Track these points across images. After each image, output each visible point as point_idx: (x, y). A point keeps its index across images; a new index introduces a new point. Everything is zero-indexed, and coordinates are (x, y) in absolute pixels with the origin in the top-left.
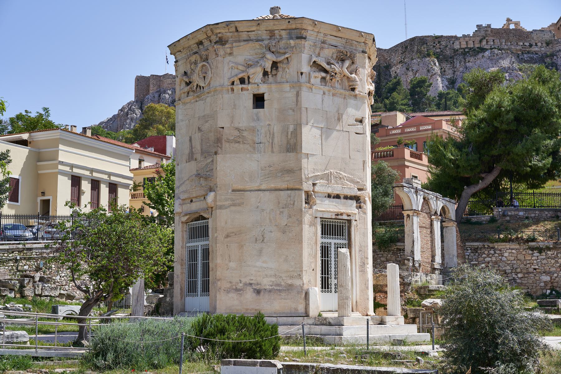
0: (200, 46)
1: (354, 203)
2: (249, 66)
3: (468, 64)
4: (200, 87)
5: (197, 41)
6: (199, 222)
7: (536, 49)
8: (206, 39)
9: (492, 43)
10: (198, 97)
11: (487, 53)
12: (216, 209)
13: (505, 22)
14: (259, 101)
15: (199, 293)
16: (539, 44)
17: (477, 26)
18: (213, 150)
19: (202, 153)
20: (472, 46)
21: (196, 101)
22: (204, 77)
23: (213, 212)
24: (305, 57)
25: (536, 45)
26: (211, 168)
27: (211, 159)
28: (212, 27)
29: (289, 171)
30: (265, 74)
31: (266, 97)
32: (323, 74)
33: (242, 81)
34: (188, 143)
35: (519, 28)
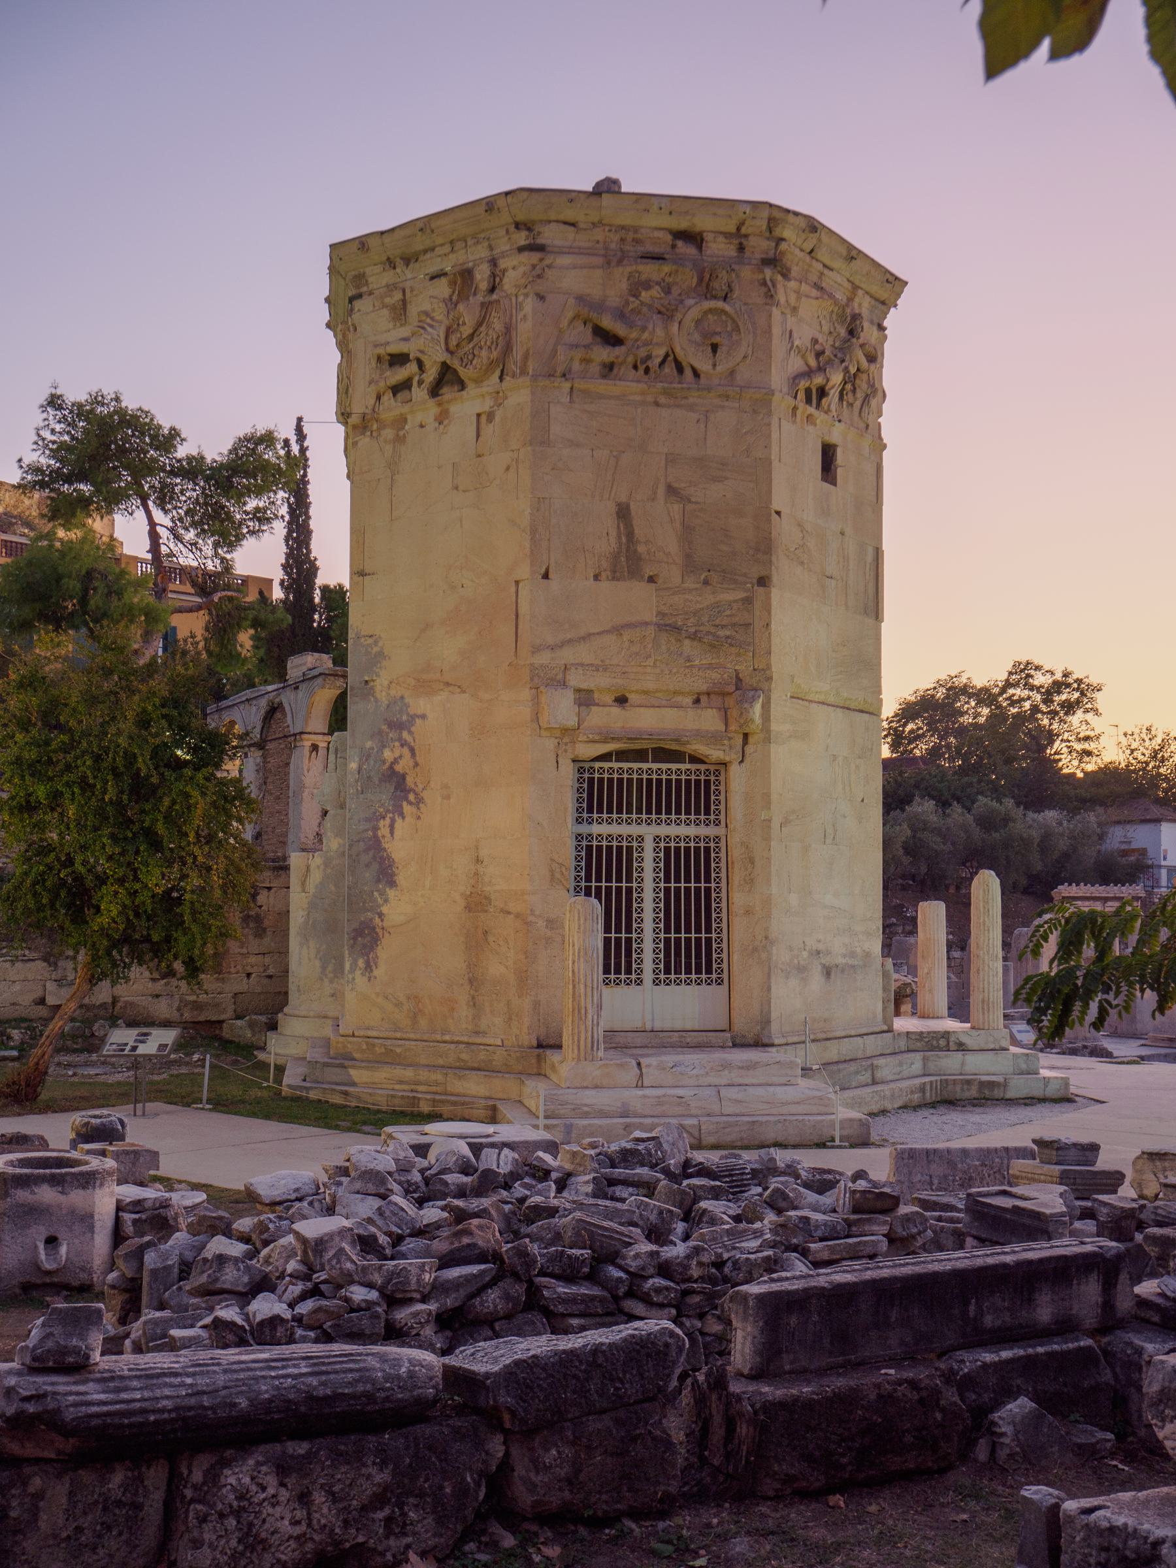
0: (680, 243)
4: (680, 369)
5: (683, 224)
6: (645, 766)
8: (727, 235)
10: (666, 393)
12: (768, 740)
15: (648, 976)
18: (755, 572)
19: (690, 565)
21: (657, 404)
22: (715, 348)
23: (749, 749)
26: (734, 620)
27: (743, 595)
28: (777, 214)
34: (610, 523)
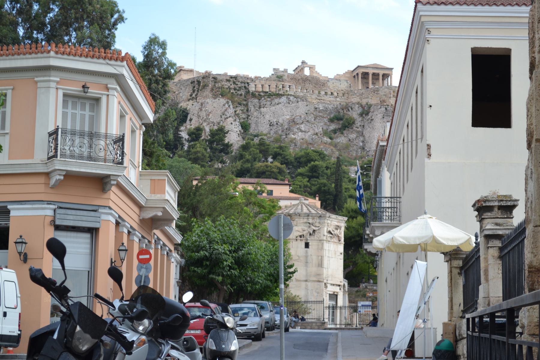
1: (338, 288)
2: (304, 231)
3: (262, 109)
7: (332, 99)
9: (288, 89)
11: (284, 99)
13: (300, 64)
14: (307, 245)
16: (335, 94)
17: (274, 69)
20: (267, 90)
24: (326, 229)
25: (332, 94)
29: (319, 275)
30: (310, 234)
31: (310, 244)
32: (331, 235)
33: (301, 236)
35: (315, 75)
